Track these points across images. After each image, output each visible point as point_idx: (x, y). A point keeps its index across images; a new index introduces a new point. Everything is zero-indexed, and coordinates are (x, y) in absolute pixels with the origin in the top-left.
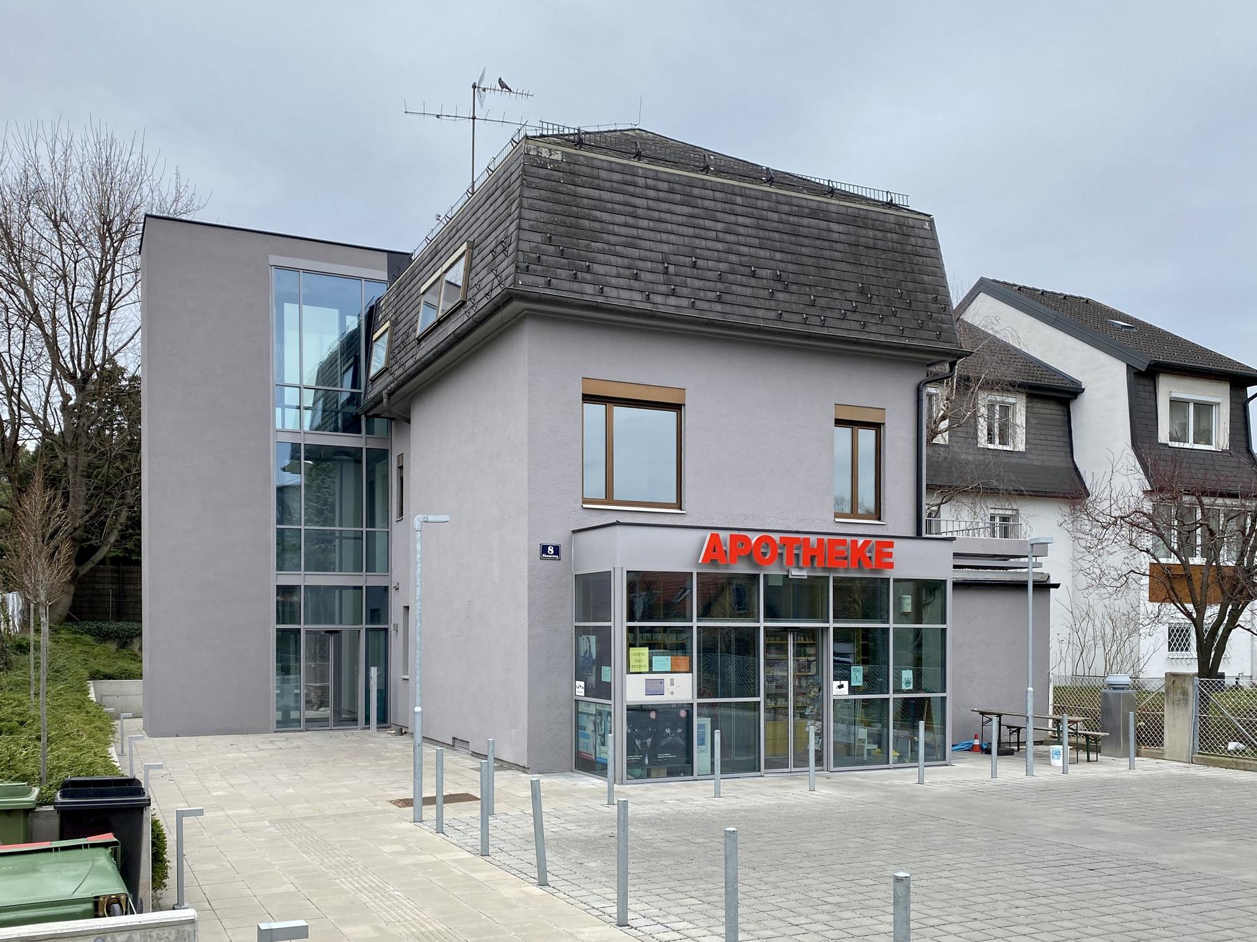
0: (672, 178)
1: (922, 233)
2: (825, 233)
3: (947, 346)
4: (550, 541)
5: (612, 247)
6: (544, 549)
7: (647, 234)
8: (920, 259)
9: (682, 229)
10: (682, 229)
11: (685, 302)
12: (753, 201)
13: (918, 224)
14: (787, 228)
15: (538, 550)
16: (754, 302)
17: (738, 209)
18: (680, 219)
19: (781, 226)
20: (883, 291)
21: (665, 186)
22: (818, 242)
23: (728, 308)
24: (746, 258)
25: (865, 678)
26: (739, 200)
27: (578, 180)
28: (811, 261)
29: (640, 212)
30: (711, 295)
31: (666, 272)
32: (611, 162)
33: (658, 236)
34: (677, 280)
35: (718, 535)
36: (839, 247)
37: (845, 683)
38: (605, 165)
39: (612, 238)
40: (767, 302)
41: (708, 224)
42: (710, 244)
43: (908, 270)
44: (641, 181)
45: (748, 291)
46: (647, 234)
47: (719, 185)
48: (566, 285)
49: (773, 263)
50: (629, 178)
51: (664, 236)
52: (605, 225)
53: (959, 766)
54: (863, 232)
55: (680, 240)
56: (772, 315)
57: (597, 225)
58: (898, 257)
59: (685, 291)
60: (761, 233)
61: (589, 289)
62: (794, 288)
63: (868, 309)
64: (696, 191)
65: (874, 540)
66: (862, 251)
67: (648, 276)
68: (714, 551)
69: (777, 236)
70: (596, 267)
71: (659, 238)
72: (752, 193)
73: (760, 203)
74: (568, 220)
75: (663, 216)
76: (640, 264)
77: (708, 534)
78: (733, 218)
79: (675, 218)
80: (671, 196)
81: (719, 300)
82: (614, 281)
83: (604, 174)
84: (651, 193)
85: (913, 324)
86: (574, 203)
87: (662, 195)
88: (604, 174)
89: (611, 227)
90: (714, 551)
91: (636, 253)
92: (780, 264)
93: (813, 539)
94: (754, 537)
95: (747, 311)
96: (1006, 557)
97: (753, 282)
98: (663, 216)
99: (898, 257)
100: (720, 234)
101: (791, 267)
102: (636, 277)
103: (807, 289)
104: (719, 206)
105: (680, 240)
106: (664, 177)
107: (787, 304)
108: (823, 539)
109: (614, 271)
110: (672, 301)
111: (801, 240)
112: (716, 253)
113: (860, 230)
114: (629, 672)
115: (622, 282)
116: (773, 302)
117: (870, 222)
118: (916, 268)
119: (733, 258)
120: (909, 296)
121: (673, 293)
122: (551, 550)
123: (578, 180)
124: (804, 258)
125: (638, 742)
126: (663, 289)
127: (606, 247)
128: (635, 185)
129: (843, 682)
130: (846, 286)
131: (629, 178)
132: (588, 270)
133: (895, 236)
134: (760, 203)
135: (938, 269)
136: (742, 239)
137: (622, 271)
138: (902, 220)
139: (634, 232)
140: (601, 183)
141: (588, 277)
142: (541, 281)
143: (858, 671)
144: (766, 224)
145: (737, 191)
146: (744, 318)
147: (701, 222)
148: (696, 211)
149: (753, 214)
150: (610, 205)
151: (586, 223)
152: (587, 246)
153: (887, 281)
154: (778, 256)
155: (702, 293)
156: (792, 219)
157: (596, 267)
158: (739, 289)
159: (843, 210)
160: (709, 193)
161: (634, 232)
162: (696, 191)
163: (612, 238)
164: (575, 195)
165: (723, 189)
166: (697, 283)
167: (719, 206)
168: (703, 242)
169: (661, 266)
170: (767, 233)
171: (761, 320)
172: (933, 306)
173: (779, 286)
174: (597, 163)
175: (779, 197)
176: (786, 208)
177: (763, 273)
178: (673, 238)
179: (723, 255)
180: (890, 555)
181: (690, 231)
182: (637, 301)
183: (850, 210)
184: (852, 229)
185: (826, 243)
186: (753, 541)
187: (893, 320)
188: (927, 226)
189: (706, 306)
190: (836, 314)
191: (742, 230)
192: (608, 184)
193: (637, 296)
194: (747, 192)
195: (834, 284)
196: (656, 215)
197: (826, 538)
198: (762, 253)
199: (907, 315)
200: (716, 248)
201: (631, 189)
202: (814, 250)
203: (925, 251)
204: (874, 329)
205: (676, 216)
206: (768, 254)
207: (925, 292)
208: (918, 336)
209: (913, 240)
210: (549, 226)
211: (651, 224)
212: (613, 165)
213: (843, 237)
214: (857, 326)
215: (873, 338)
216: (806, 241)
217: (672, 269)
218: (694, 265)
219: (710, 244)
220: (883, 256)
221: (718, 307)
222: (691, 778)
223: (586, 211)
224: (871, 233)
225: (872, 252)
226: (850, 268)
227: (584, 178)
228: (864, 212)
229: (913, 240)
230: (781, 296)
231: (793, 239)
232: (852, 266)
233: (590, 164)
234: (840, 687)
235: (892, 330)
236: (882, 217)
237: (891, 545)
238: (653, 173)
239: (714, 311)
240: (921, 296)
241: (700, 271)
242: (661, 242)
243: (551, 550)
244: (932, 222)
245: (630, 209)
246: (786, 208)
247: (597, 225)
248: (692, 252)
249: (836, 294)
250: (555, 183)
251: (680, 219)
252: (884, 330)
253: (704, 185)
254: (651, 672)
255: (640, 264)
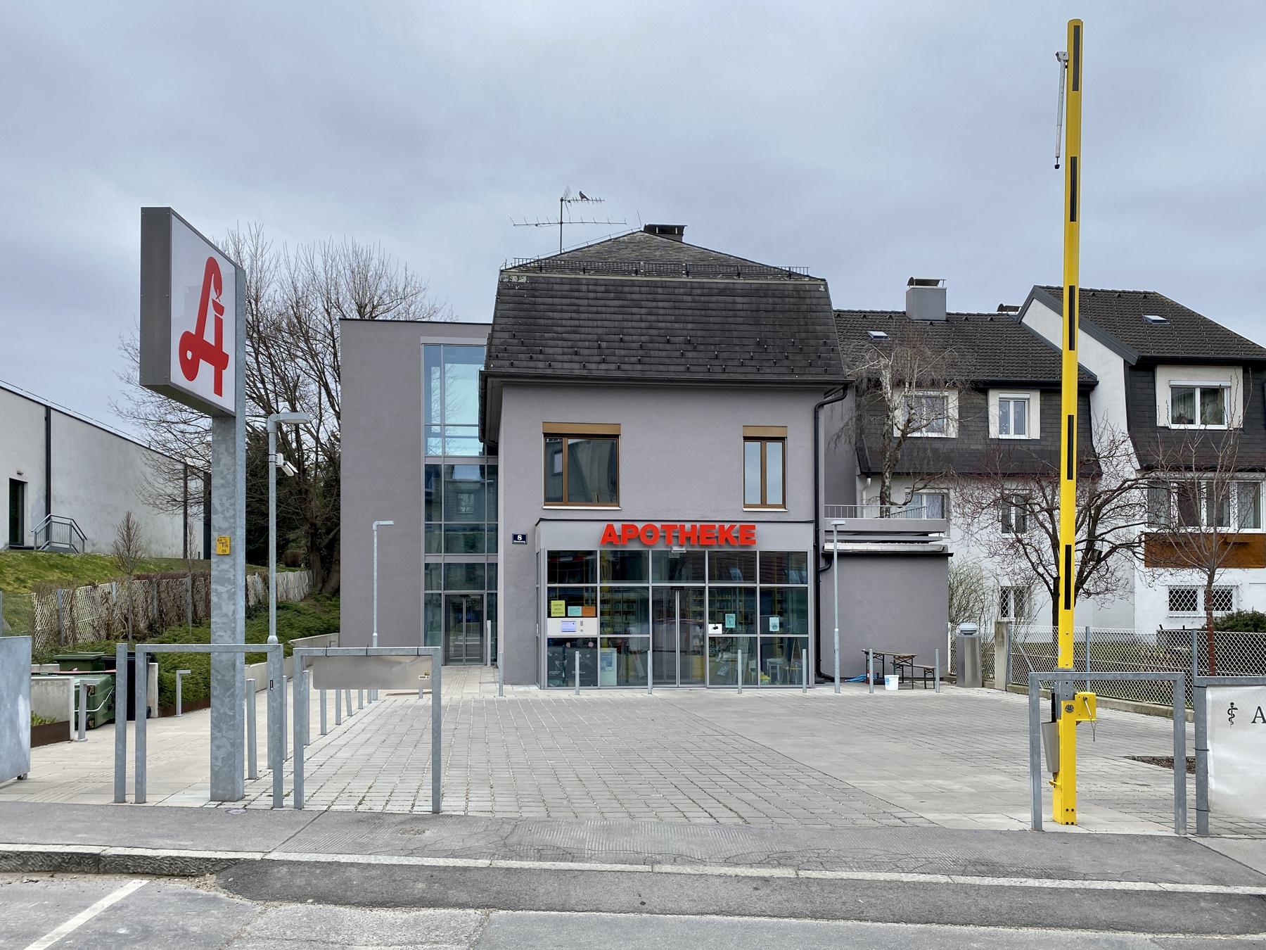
0: (608, 283)
1: (817, 294)
2: (730, 305)
3: (833, 378)
4: (520, 532)
5: (560, 335)
6: (515, 537)
7: (586, 323)
8: (814, 314)
9: (613, 317)
10: (613, 317)
11: (613, 366)
12: (671, 290)
13: (814, 288)
14: (699, 306)
15: (511, 538)
16: (668, 361)
17: (659, 297)
18: (613, 309)
19: (694, 304)
20: (778, 342)
21: (603, 288)
22: (724, 312)
23: (647, 367)
24: (663, 331)
25: (781, 625)
26: (660, 290)
27: (537, 294)
28: (716, 327)
29: (582, 309)
30: (633, 360)
31: (599, 347)
32: (562, 278)
33: (595, 324)
34: (607, 351)
35: (612, 525)
36: (742, 314)
37: (720, 626)
38: (558, 281)
39: (560, 329)
40: (678, 360)
41: (634, 310)
42: (635, 324)
43: (802, 323)
44: (584, 288)
45: (664, 354)
46: (586, 323)
47: (645, 283)
48: (525, 364)
49: (685, 332)
50: (575, 287)
51: (600, 323)
52: (555, 321)
53: (818, 688)
54: (764, 300)
55: (612, 324)
56: (682, 368)
57: (549, 322)
58: (794, 315)
59: (613, 358)
60: (677, 312)
61: (541, 365)
62: (702, 347)
63: (764, 356)
64: (626, 289)
65: (738, 525)
66: (762, 314)
67: (586, 352)
68: (698, 537)
69: (690, 312)
70: (547, 350)
71: (595, 325)
72: (671, 284)
73: (677, 291)
74: (528, 321)
75: (599, 309)
76: (580, 344)
77: (605, 524)
78: (654, 304)
79: (608, 310)
80: (606, 295)
81: (640, 362)
82: (560, 358)
83: (556, 287)
84: (592, 295)
85: (804, 363)
86: (533, 309)
87: (599, 295)
88: (556, 287)
89: (560, 321)
90: (707, 538)
91: (577, 337)
92: (691, 332)
93: (688, 526)
94: (640, 526)
95: (662, 368)
96: (926, 534)
97: (668, 347)
98: (599, 309)
99: (794, 315)
100: (643, 317)
101: (699, 333)
102: (576, 353)
103: (713, 347)
104: (644, 297)
105: (612, 324)
106: (602, 282)
107: (695, 360)
108: (696, 526)
109: (560, 350)
110: (603, 366)
111: (709, 312)
112: (639, 330)
113: (761, 299)
114: (549, 616)
115: (565, 357)
116: (683, 360)
117: (770, 292)
118: (810, 321)
119: (653, 332)
120: (801, 344)
121: (604, 361)
122: (520, 537)
123: (537, 294)
124: (711, 325)
125: (557, 663)
126: (597, 359)
127: (555, 335)
128: (579, 291)
129: (717, 625)
130: (746, 342)
131: (575, 287)
132: (541, 352)
133: (792, 300)
134: (677, 291)
135: (830, 320)
136: (661, 318)
137: (566, 350)
138: (799, 286)
139: (577, 323)
140: (554, 293)
141: (541, 357)
142: (507, 363)
143: (731, 617)
144: (682, 305)
145: (659, 284)
146: (659, 373)
147: (629, 310)
148: (625, 302)
149: (671, 299)
150: (560, 307)
151: (542, 321)
152: (541, 336)
153: (783, 334)
154: (690, 326)
155: (626, 359)
156: (703, 299)
157: (547, 350)
158: (656, 353)
159: (747, 287)
160: (637, 289)
161: (577, 323)
162: (626, 289)
163: (560, 329)
164: (535, 304)
165: (647, 284)
166: (623, 352)
167: (644, 297)
168: (630, 323)
169: (596, 344)
170: (681, 311)
171: (673, 374)
172: (823, 349)
173: (689, 347)
174: (552, 280)
175: (693, 284)
176: (699, 291)
177: (677, 339)
178: (606, 323)
179: (644, 331)
180: (753, 535)
181: (620, 317)
182: (577, 370)
183: (753, 286)
184: (754, 299)
185: (731, 313)
186: (640, 529)
187: (786, 363)
188: (822, 289)
189: (629, 367)
190: (736, 363)
191: (662, 311)
192: (559, 293)
193: (576, 366)
194: (668, 284)
195: (736, 341)
196: (594, 309)
197: (698, 524)
198: (677, 325)
199: (798, 357)
200: (640, 326)
201: (576, 294)
202: (720, 319)
203: (819, 308)
204: (768, 370)
205: (610, 308)
206: (681, 325)
207: (817, 338)
208: (807, 372)
209: (808, 301)
210: (515, 327)
211: (590, 316)
212: (564, 280)
213: (745, 306)
214: (754, 370)
215: (767, 377)
216: (714, 313)
217: (604, 345)
218: (621, 340)
219: (635, 324)
220: (781, 316)
221: (639, 367)
222: (596, 687)
223: (542, 313)
224: (770, 300)
225: (771, 314)
226: (750, 328)
227: (542, 292)
228: (697, 284)
229: (808, 301)
230: (690, 355)
231: (703, 312)
232: (752, 326)
233: (547, 281)
234: (716, 628)
235: (783, 370)
236: (781, 287)
237: (754, 527)
238: (594, 281)
239: (635, 371)
240: (812, 342)
241: (626, 344)
242: (597, 327)
243: (520, 537)
244: (826, 285)
245: (575, 308)
246: (699, 291)
247: (549, 322)
248: (621, 331)
249: (737, 348)
250: (520, 298)
251: (613, 309)
252: (777, 370)
253: (633, 284)
254: (566, 616)
255: (580, 344)
